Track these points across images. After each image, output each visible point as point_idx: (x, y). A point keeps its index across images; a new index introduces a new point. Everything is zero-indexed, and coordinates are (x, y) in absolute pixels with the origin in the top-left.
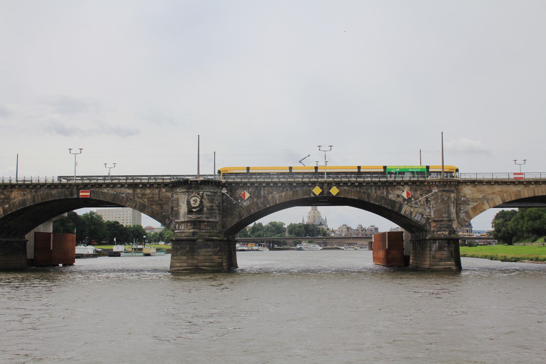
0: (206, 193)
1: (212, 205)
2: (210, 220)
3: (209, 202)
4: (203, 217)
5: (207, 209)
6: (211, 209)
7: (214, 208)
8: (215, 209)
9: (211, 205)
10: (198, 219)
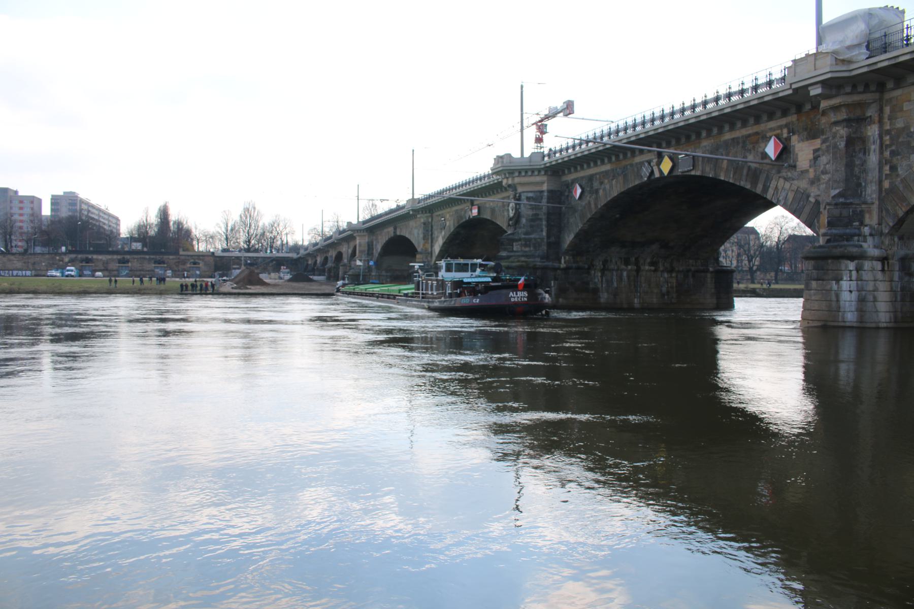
0: (525, 194)
2: (532, 236)
4: (520, 232)
5: (527, 220)
6: (535, 218)
7: (540, 217)
8: (541, 219)
9: (535, 212)
10: (511, 237)
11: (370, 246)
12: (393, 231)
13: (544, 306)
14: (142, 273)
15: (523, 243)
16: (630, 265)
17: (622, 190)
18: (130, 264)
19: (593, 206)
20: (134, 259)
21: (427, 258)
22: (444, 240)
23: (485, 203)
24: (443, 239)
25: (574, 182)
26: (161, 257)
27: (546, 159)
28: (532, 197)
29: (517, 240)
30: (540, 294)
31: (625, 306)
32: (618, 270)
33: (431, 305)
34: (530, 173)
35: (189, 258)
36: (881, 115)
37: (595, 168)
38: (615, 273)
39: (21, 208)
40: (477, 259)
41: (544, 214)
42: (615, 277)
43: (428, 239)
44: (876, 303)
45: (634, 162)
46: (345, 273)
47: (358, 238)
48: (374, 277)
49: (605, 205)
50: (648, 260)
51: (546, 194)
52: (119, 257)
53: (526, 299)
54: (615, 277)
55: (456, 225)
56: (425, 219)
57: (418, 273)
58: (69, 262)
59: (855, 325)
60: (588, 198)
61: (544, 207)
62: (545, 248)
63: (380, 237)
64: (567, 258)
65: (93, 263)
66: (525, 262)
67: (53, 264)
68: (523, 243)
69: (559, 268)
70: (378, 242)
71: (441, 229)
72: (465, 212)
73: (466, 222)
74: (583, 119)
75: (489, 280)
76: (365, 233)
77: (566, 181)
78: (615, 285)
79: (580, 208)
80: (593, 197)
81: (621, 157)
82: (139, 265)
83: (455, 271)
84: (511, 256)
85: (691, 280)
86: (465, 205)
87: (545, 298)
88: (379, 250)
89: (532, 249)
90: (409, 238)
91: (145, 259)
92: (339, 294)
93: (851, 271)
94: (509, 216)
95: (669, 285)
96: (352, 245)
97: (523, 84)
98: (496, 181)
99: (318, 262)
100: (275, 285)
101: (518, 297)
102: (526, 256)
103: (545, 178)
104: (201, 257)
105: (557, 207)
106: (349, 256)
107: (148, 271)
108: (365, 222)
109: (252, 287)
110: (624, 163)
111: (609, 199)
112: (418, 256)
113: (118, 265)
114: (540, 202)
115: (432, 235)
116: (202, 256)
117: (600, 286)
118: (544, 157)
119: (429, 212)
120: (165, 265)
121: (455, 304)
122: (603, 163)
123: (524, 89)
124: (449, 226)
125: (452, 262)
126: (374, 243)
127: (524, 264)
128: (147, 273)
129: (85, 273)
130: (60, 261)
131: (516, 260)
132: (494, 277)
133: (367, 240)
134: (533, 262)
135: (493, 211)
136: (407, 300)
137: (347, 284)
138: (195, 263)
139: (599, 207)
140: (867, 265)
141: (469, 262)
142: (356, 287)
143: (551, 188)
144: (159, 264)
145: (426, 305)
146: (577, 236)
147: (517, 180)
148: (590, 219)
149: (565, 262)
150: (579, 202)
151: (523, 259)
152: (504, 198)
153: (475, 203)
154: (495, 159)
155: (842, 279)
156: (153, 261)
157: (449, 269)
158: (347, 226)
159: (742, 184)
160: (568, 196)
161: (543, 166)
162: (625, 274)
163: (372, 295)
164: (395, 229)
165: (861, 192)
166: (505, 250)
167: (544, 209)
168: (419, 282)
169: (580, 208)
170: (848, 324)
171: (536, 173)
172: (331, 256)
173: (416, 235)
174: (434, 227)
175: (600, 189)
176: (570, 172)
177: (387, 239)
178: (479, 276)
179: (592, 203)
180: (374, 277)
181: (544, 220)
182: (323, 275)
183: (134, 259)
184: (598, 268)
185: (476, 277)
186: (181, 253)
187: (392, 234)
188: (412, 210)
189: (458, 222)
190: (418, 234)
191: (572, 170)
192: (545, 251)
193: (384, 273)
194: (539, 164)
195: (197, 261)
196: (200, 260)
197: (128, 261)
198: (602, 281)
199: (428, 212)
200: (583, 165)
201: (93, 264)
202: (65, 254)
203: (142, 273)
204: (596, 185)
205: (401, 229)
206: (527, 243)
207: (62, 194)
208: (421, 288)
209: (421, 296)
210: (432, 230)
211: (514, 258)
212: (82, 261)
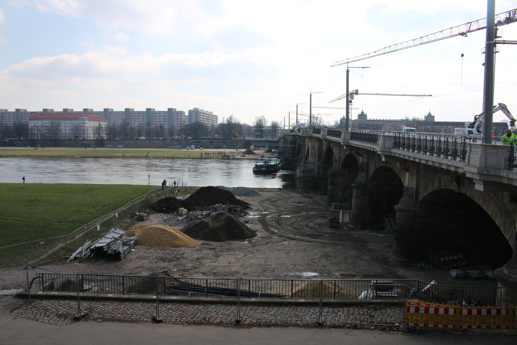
39: (177, 119)
58: (193, 143)
116: (241, 140)
129: (198, 146)
138: (238, 143)
140: (301, 167)
144: (225, 143)
186: (233, 139)
197: (213, 142)
202: (191, 140)
207: (193, 109)
212: (197, 142)
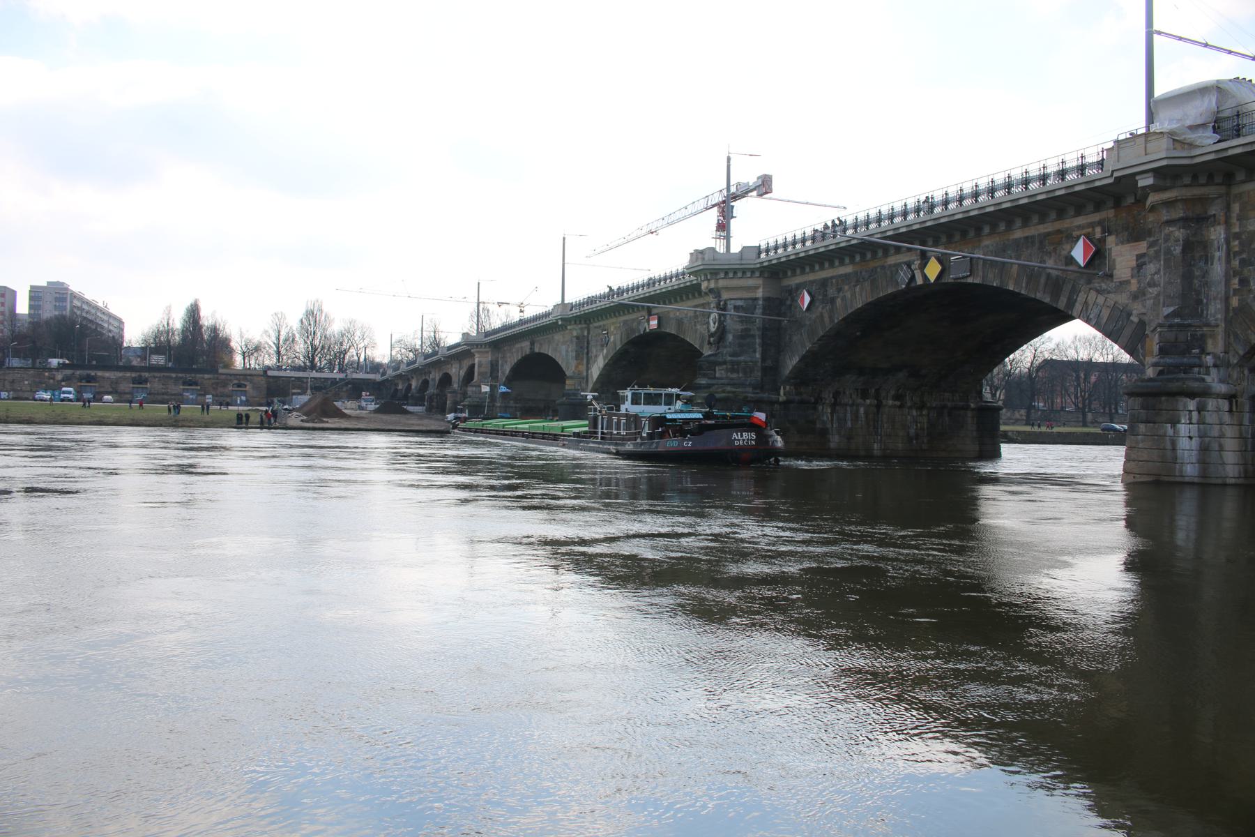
0: (733, 302)
1: (748, 326)
2: (742, 358)
3: (739, 321)
5: (733, 336)
6: (745, 335)
7: (752, 333)
8: (753, 336)
9: (745, 327)
10: (712, 358)
11: (494, 367)
12: (529, 347)
13: (776, 453)
14: (166, 397)
15: (729, 367)
16: (868, 399)
17: (870, 300)
18: (148, 385)
19: (827, 319)
20: (155, 377)
21: (580, 384)
22: (607, 361)
23: (668, 312)
24: (604, 360)
25: (799, 287)
26: (193, 375)
27: (763, 256)
28: (742, 306)
29: (720, 364)
30: (771, 436)
31: (862, 453)
32: (852, 405)
33: (620, 448)
34: (740, 274)
35: (232, 378)
36: (1228, 214)
37: (831, 271)
38: (848, 408)
40: (672, 388)
41: (759, 329)
42: (849, 415)
43: (582, 359)
44: (1222, 452)
45: (886, 264)
46: (456, 403)
47: (477, 355)
48: (498, 409)
49: (844, 319)
50: (892, 392)
51: (760, 302)
52: (134, 375)
53: (753, 443)
54: (849, 415)
55: (625, 341)
56: (579, 331)
57: (593, 405)
59: (1196, 480)
60: (820, 309)
61: (757, 320)
62: (758, 374)
63: (508, 355)
64: (788, 387)
65: (98, 382)
66: (734, 392)
67: (41, 383)
68: (729, 367)
69: (777, 402)
70: (506, 362)
71: (602, 346)
72: (639, 323)
73: (641, 336)
74: (807, 203)
75: (700, 416)
76: (487, 350)
77: (789, 285)
78: (849, 424)
79: (808, 323)
80: (828, 308)
81: (869, 256)
82: (161, 386)
83: (644, 404)
84: (713, 385)
85: (947, 419)
86: (638, 315)
87: (777, 441)
88: (507, 372)
89: (741, 375)
90: (554, 357)
91: (171, 378)
92: (456, 431)
93: (1191, 411)
94: (709, 331)
95: (919, 425)
96: (466, 364)
97: (730, 155)
98: (688, 284)
99: (413, 387)
100: (358, 418)
101: (744, 440)
102: (733, 385)
103: (760, 282)
104: (249, 377)
105: (775, 320)
106: (461, 379)
107: (174, 395)
108: (487, 334)
109: (330, 420)
110: (872, 264)
111: (850, 311)
112: (567, 382)
113: (131, 385)
114: (753, 314)
115: (588, 353)
116: (250, 375)
117: (829, 426)
118: (760, 253)
119: (585, 323)
120: (199, 388)
121: (657, 447)
122: (842, 263)
123: (731, 162)
124: (614, 342)
125: (640, 391)
126: (500, 362)
127: (731, 395)
128: (173, 397)
130: (49, 378)
131: (720, 390)
132: (706, 412)
133: (490, 359)
134: (743, 392)
135: (680, 322)
136: (581, 442)
137: (469, 418)
138: (239, 386)
139: (836, 321)
141: (663, 391)
142: (484, 422)
143: (767, 295)
144: (191, 385)
145: (612, 449)
146: (803, 359)
147: (722, 283)
148: (823, 336)
149: (785, 394)
150: (807, 314)
151: (729, 388)
152: (696, 306)
153: (654, 311)
154: (691, 254)
155: (1179, 422)
156: (181, 381)
157: (635, 401)
158: (463, 338)
159: (1039, 296)
160: (791, 305)
161: (758, 266)
162: (862, 410)
163: (515, 434)
164: (532, 344)
165: (1202, 311)
166: (705, 376)
167: (758, 323)
168: (595, 419)
169: (808, 323)
170: (1187, 479)
171: (749, 274)
172: (434, 380)
173: (564, 353)
174: (592, 343)
175: (838, 297)
176: (794, 274)
177: (520, 358)
178: (682, 411)
179: (826, 316)
180: (498, 409)
181: (757, 337)
182: (420, 405)
183: (155, 377)
184: (827, 402)
185: (676, 412)
186: (221, 371)
187: (528, 352)
188: (561, 319)
189: (628, 338)
190: (567, 351)
191: (798, 271)
192: (759, 379)
193: (512, 403)
194: (752, 262)
195: (243, 382)
196: (246, 380)
197: (146, 381)
198: (832, 420)
199: (583, 322)
200: (814, 266)
201: (97, 384)
203: (166, 397)
204: (831, 292)
205: (541, 344)
206: (734, 367)
207: (45, 284)
208: (600, 426)
209: (599, 435)
210: (588, 347)
211: (716, 386)
212: (81, 379)
